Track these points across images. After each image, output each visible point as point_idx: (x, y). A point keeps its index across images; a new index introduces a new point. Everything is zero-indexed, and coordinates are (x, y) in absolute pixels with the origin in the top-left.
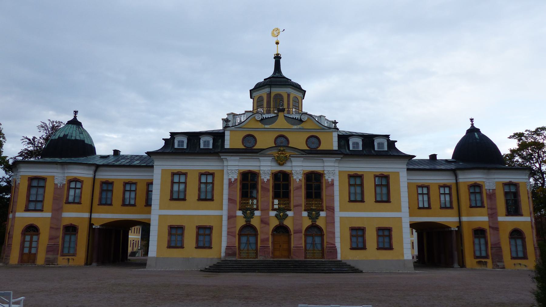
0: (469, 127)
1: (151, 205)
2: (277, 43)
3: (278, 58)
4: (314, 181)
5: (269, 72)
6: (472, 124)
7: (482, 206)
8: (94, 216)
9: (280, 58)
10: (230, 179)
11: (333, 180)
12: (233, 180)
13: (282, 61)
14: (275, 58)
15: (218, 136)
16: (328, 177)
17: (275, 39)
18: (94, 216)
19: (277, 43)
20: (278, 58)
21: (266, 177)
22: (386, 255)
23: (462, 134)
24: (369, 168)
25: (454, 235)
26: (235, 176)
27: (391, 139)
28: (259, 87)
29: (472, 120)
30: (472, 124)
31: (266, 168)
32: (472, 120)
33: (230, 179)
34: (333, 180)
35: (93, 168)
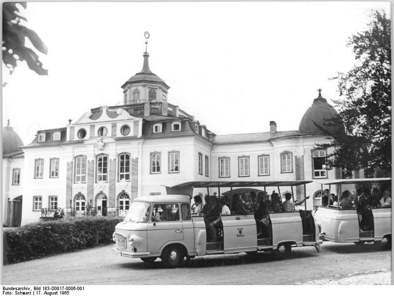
0: (317, 96)
2: (146, 43)
3: (146, 56)
4: (125, 159)
5: (140, 69)
6: (320, 95)
7: (292, 172)
9: (149, 56)
11: (137, 158)
12: (69, 162)
13: (150, 59)
14: (144, 56)
15: (63, 132)
16: (133, 156)
17: (146, 40)
19: (146, 43)
20: (146, 56)
21: (91, 158)
23: (309, 104)
26: (71, 159)
29: (320, 90)
30: (320, 95)
31: (90, 151)
32: (320, 90)
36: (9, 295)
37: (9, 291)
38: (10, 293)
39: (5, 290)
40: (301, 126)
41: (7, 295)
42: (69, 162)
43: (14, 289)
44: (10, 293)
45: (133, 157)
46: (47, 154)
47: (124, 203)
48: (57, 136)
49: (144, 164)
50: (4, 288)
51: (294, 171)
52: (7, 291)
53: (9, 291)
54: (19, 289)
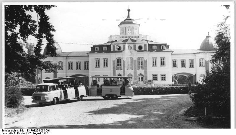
1: (89, 69)
7: (204, 66)
8: (67, 74)
10: (113, 61)
11: (146, 60)
12: (114, 60)
15: (109, 47)
18: (67, 74)
22: (164, 82)
24: (158, 55)
25: (194, 77)
27: (167, 45)
28: (122, 23)
29: (208, 32)
32: (208, 32)
33: (113, 61)
34: (146, 60)
35: (65, 57)
36: (6, 134)
37: (6, 132)
38: (6, 133)
39: (3, 132)
40: (200, 48)
41: (4, 134)
42: (114, 60)
43: (8, 131)
44: (6, 133)
45: (134, 59)
46: (101, 56)
47: (141, 78)
48: (105, 48)
49: (150, 63)
50: (2, 130)
51: (205, 66)
52: (4, 132)
53: (6, 132)
54: (12, 131)
